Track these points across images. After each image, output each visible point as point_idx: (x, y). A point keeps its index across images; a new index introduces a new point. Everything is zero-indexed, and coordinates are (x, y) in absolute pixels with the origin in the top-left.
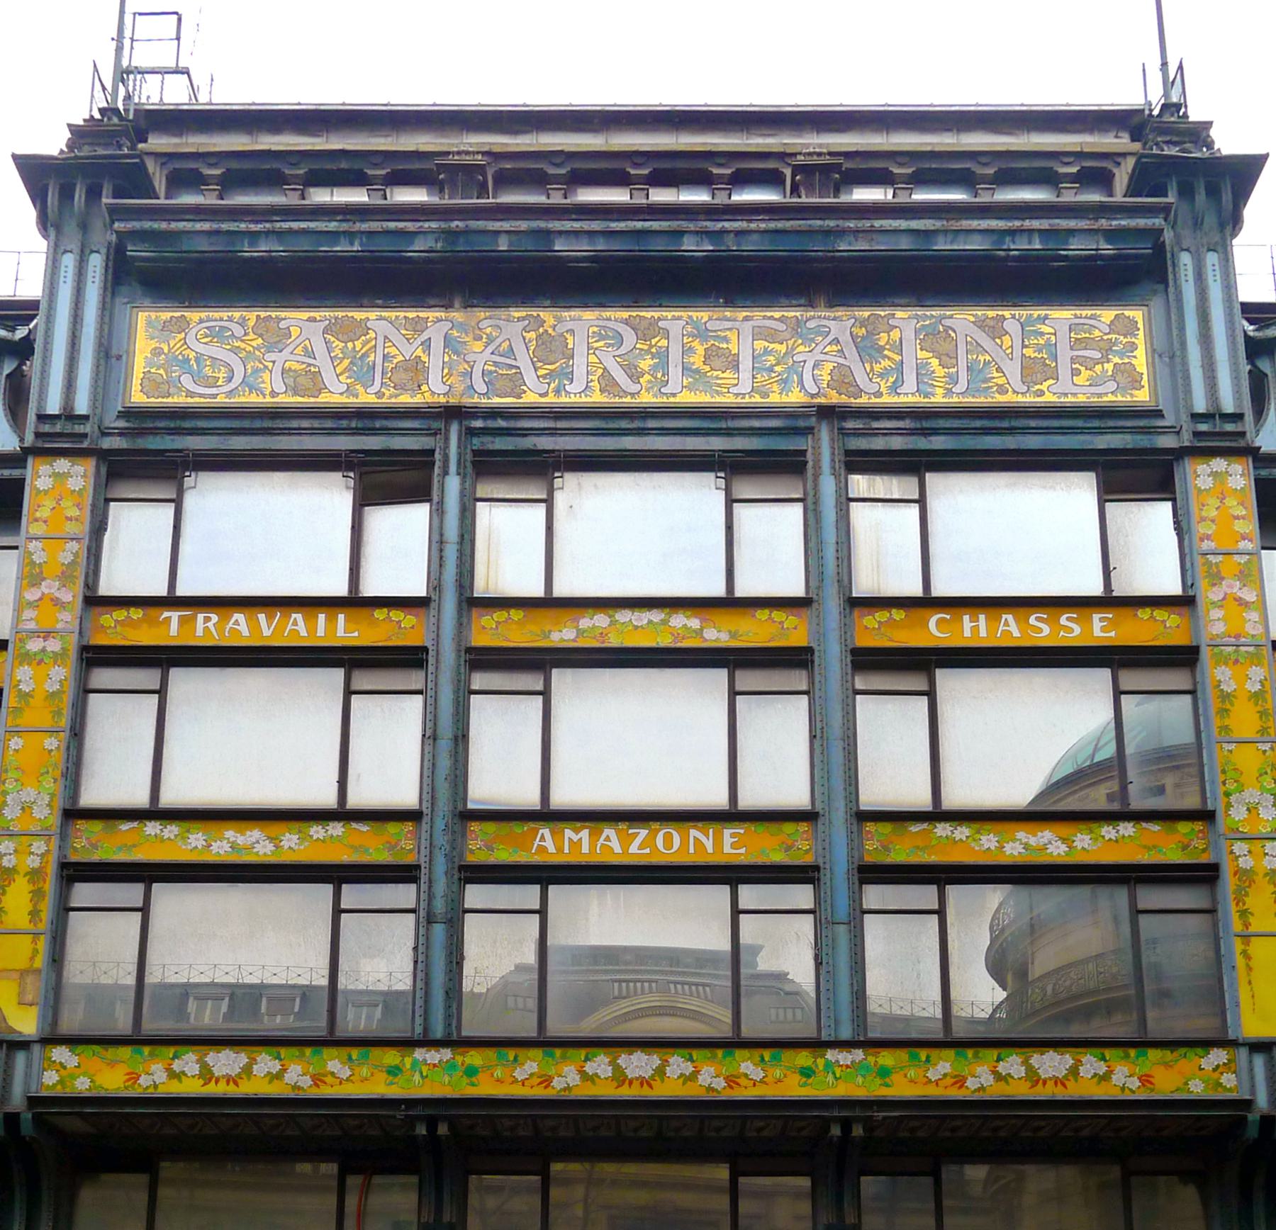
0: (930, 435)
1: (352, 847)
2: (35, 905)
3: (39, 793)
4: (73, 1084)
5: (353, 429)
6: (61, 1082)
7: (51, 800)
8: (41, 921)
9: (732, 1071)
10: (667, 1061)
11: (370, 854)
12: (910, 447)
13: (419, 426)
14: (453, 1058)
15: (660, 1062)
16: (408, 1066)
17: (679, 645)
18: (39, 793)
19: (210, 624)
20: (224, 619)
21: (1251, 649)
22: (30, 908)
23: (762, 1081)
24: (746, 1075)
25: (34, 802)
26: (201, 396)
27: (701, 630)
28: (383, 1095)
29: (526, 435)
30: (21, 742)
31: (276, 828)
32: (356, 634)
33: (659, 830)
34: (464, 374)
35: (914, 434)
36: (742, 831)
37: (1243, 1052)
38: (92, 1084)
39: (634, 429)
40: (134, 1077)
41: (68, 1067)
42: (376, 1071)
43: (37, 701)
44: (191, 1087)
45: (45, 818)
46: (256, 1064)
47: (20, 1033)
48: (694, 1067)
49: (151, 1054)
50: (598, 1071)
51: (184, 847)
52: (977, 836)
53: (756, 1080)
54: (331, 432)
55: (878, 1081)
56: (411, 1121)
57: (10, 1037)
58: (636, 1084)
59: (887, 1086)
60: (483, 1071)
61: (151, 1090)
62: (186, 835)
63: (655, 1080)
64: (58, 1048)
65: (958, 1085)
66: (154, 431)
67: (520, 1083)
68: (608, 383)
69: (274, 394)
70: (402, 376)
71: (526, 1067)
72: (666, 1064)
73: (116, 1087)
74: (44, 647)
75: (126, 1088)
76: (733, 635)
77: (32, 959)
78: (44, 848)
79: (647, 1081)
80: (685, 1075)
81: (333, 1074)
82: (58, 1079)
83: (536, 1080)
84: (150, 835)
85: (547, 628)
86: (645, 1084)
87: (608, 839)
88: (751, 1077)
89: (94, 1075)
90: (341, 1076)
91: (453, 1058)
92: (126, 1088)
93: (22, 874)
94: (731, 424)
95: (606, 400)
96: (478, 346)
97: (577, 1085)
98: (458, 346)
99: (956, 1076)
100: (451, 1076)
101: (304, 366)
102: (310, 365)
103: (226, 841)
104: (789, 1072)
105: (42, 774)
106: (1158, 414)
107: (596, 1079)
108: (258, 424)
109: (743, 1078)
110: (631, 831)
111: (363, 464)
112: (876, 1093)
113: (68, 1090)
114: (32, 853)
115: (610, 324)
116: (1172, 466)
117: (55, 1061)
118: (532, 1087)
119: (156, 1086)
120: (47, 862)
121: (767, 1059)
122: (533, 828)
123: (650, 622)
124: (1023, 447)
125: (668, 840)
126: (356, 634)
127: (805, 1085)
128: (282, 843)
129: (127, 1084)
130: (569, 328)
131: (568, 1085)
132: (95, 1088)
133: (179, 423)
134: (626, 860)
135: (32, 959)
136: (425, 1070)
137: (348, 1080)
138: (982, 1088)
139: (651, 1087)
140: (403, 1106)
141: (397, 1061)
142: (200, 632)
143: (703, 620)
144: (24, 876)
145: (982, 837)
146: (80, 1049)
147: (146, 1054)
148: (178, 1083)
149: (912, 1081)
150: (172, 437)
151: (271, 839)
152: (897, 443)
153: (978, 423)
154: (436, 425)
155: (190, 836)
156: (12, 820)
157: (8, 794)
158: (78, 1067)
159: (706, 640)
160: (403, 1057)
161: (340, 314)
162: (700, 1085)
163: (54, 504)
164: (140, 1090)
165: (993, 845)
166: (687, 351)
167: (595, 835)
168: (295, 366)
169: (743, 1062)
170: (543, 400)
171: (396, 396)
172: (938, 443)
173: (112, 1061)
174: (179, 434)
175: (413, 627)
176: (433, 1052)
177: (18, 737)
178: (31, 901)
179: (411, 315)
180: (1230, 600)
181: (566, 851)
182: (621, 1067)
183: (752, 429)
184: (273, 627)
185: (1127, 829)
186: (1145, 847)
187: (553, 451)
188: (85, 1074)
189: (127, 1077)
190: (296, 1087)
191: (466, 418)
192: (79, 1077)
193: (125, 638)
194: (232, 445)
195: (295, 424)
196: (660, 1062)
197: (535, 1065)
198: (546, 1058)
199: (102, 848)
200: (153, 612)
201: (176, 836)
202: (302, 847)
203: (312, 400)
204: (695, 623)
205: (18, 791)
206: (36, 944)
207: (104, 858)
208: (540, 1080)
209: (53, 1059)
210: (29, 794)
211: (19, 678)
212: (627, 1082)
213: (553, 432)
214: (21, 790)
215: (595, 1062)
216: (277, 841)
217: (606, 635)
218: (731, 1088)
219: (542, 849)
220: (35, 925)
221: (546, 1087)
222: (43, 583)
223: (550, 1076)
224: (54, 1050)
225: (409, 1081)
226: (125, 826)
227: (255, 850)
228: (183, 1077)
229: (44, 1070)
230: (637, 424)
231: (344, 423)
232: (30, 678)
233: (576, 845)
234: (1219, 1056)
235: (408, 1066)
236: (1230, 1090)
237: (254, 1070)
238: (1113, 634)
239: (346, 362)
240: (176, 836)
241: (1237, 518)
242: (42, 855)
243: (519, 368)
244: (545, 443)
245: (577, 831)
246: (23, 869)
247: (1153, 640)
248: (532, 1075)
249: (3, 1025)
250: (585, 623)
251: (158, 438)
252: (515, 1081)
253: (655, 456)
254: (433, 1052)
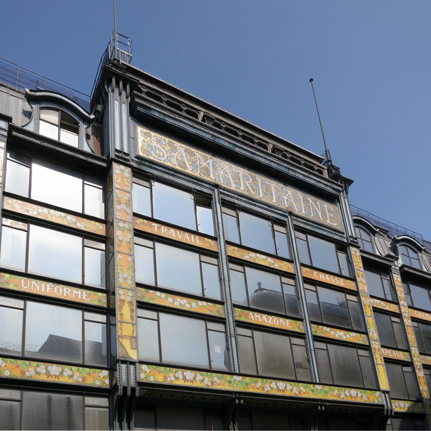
0: (308, 225)
1: (209, 310)
2: (132, 314)
3: (128, 275)
4: (150, 379)
5: (193, 182)
6: (146, 377)
7: (132, 279)
8: (134, 320)
10: (286, 385)
11: (213, 313)
12: (305, 227)
13: (208, 187)
14: (242, 380)
16: (233, 381)
17: (270, 266)
18: (128, 275)
19: (165, 231)
20: (169, 230)
21: (366, 294)
22: (130, 315)
24: (302, 391)
25: (127, 278)
26: (157, 159)
27: (274, 263)
28: (229, 390)
29: (232, 198)
30: (121, 256)
31: (191, 300)
32: (201, 244)
33: (274, 318)
34: (218, 176)
35: (305, 224)
36: (290, 321)
37: (381, 392)
38: (155, 379)
39: (254, 204)
40: (166, 378)
41: (147, 372)
42: (226, 382)
43: (124, 243)
44: (181, 383)
45: (131, 284)
46: (197, 377)
47: (133, 359)
49: (169, 370)
51: (167, 302)
52: (331, 331)
54: (188, 181)
55: (326, 395)
56: (236, 398)
57: (130, 360)
59: (328, 396)
60: (249, 384)
61: (171, 383)
62: (167, 297)
64: (144, 365)
65: (339, 397)
66: (145, 165)
68: (248, 191)
69: (175, 165)
70: (204, 171)
71: (258, 384)
73: (161, 381)
74: (124, 226)
75: (164, 381)
76: (280, 267)
77: (133, 333)
78: (131, 295)
81: (216, 382)
82: (145, 376)
83: (261, 388)
84: (158, 296)
85: (243, 254)
87: (264, 318)
89: (155, 376)
90: (218, 383)
91: (242, 380)
92: (164, 381)
93: (127, 302)
94: (273, 210)
95: (248, 194)
96: (220, 169)
98: (216, 167)
99: (339, 395)
100: (242, 385)
101: (181, 159)
102: (182, 160)
103: (178, 302)
105: (128, 269)
106: (343, 234)
108: (171, 172)
110: (269, 317)
111: (196, 193)
112: (326, 398)
113: (148, 380)
114: (128, 296)
115: (246, 174)
116: (346, 247)
117: (143, 370)
119: (172, 382)
120: (133, 300)
121: (305, 386)
122: (248, 312)
123: (264, 258)
124: (323, 233)
125: (272, 321)
126: (201, 244)
127: (313, 394)
128: (192, 305)
129: (164, 380)
130: (238, 172)
132: (156, 381)
133: (151, 165)
134: (267, 325)
135: (133, 333)
136: (237, 382)
137: (219, 384)
138: (343, 398)
140: (234, 394)
141: (230, 379)
142: (163, 232)
143: (274, 261)
144: (128, 303)
145: (332, 332)
146: (150, 366)
147: (168, 370)
148: (177, 381)
149: (331, 395)
150: (149, 168)
151: (189, 304)
152: (302, 225)
153: (316, 225)
154: (213, 188)
155: (168, 298)
156: (121, 283)
157: (119, 274)
158: (150, 372)
159: (275, 267)
160: (231, 378)
161: (188, 148)
163: (121, 179)
164: (168, 383)
165: (334, 334)
166: (262, 187)
167: (261, 317)
168: (179, 159)
170: (235, 189)
171: (204, 177)
172: (309, 228)
173: (159, 372)
174: (151, 168)
175: (214, 245)
176: (238, 377)
177: (120, 255)
178: (130, 312)
179: (204, 154)
180: (361, 282)
181: (256, 320)
183: (276, 212)
184: (181, 235)
185: (354, 334)
186: (357, 339)
187: (238, 204)
188: (152, 375)
189: (164, 378)
190: (207, 385)
191: (219, 188)
192: (150, 376)
193: (143, 228)
194: (164, 176)
195: (180, 176)
197: (260, 383)
199: (145, 297)
200: (150, 222)
201: (165, 297)
202: (197, 308)
203: (184, 170)
204: (272, 261)
205: (122, 273)
206: (133, 328)
207: (146, 301)
208: (262, 388)
209: (143, 369)
210: (125, 275)
211: (118, 234)
213: (237, 199)
214: (123, 273)
216: (191, 304)
217: (256, 259)
219: (251, 319)
220: (132, 321)
221: (264, 390)
222: (121, 204)
224: (142, 366)
225: (234, 386)
226: (151, 291)
227: (186, 306)
228: (179, 379)
229: (141, 373)
230: (254, 203)
231: (192, 180)
232: (121, 235)
233: (258, 318)
234: (378, 393)
235: (233, 381)
236: (381, 402)
237: (197, 378)
238: (344, 285)
239: (191, 162)
240: (165, 297)
241: (359, 262)
242: (132, 297)
243: (229, 179)
244: (236, 201)
245: (258, 315)
246: (127, 301)
247: (350, 288)
248: (260, 386)
249: (127, 355)
250: (251, 255)
251: (145, 167)
252: (257, 388)
253: (257, 212)
254: (238, 377)
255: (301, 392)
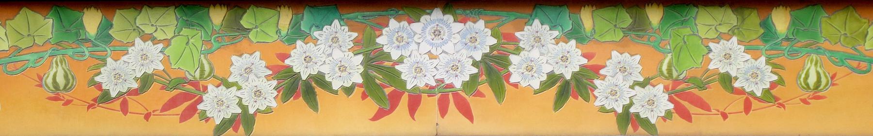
9: (688, 67)
15: (494, 41)
23: (770, 97)
24: (726, 80)
48: (584, 55)
50: (325, 69)
53: (752, 94)
58: (430, 105)
63: (480, 94)
67: (117, 104)
72: (510, 47)
79: (456, 95)
80: (561, 76)
83: (157, 96)
86: (452, 106)
88: (737, 85)
97: (269, 111)
104: (841, 71)
107: (318, 90)
109: (716, 87)
118: (147, 117)
131: (245, 108)
139: (467, 113)
162: (603, 110)
169: (717, 40)
182: (388, 56)
196: (494, 41)
198: (185, 31)
212: (405, 99)
215: (315, 41)
218: (686, 116)
221: (185, 116)
223: (195, 84)
255: (702, 94)
